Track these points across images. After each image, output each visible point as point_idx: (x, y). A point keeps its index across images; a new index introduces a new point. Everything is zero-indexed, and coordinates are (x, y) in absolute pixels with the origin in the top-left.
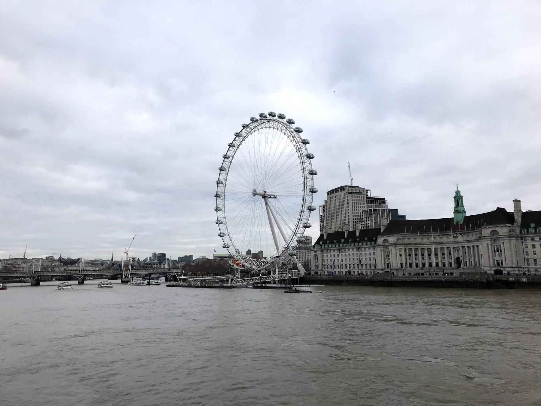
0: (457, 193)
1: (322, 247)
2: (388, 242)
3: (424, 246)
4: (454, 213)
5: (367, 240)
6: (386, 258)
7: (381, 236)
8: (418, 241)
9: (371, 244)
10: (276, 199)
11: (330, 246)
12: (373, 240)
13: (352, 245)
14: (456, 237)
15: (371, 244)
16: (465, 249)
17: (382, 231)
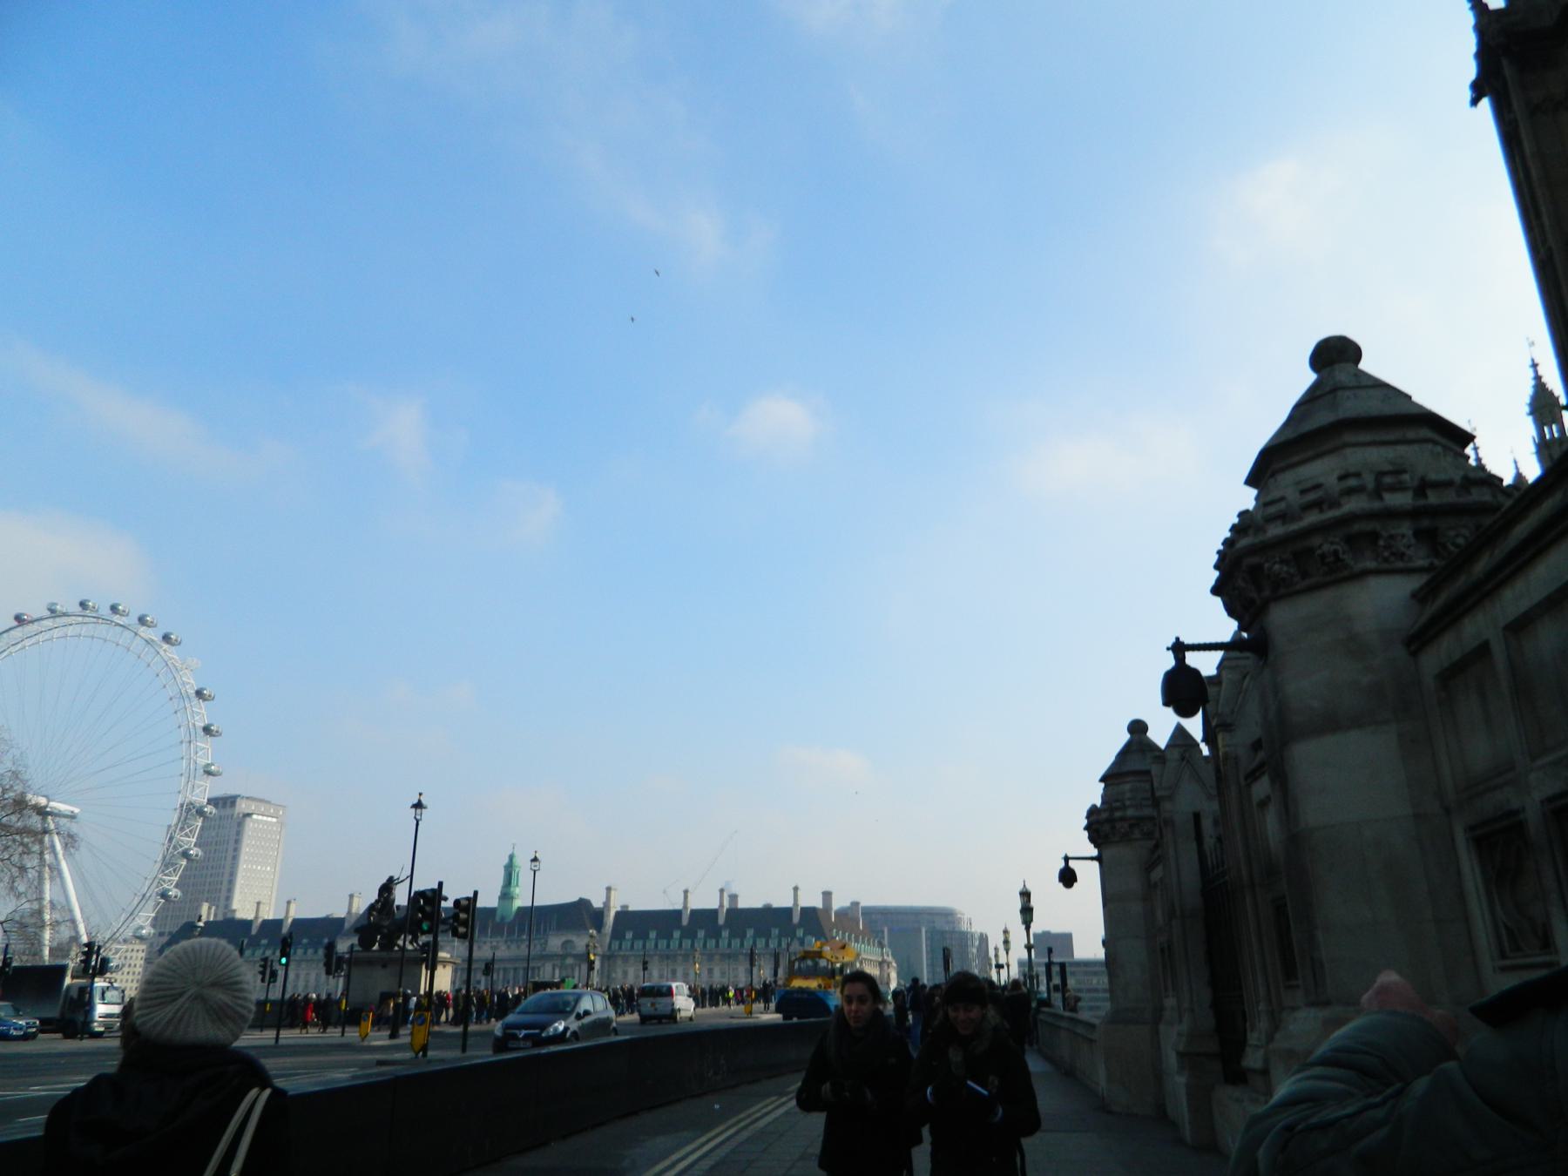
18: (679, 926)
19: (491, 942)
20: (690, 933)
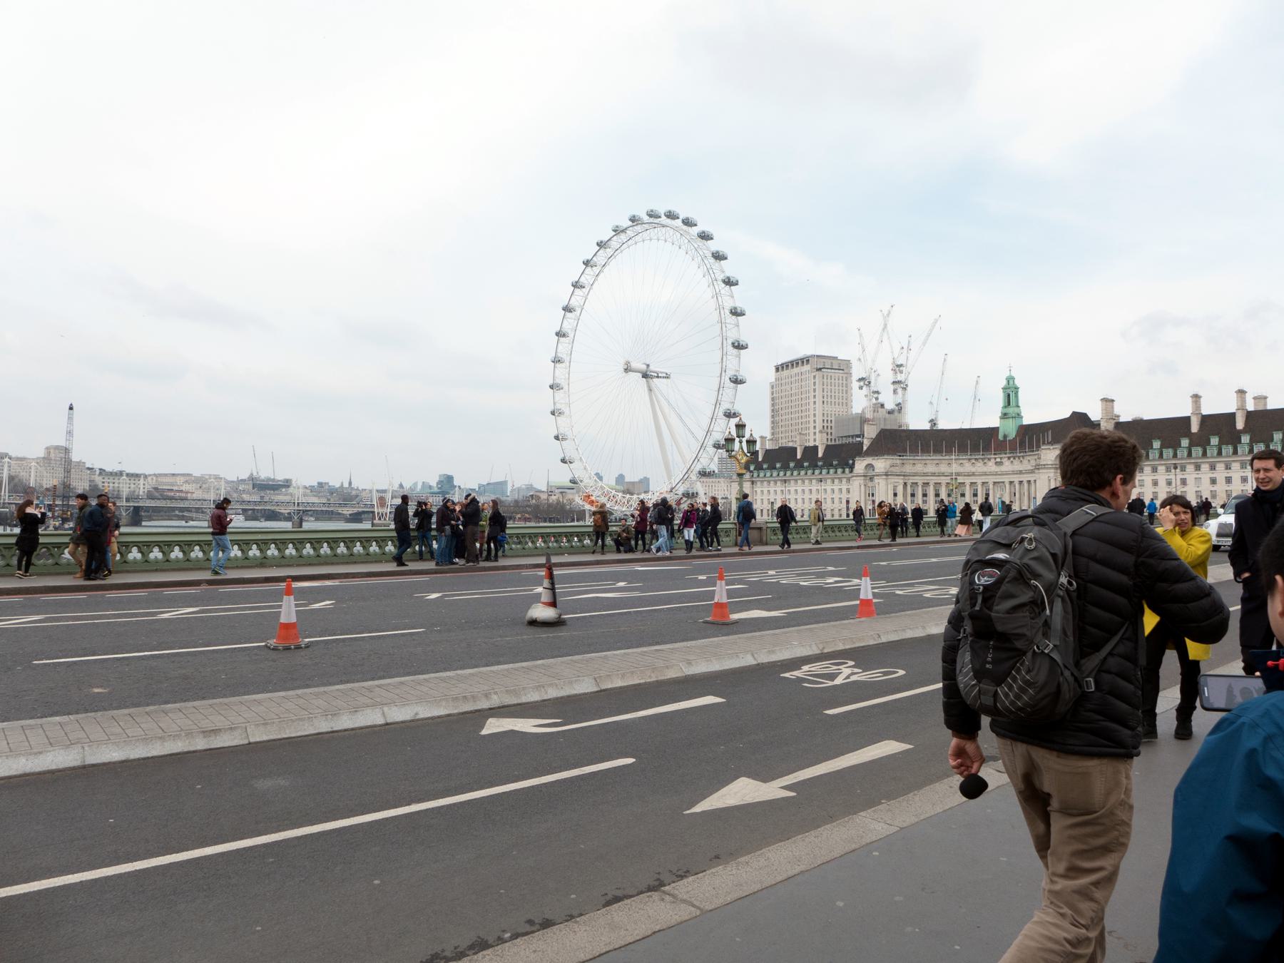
0: (1008, 381)
1: (753, 476)
2: (873, 470)
3: (940, 479)
4: (1001, 418)
5: (836, 465)
6: (869, 500)
7: (862, 459)
8: (931, 468)
9: (844, 472)
10: (668, 380)
11: (768, 474)
12: (847, 464)
13: (810, 472)
14: (1000, 464)
15: (844, 472)
16: (1015, 486)
17: (865, 448)
18: (1187, 433)
19: (995, 458)
20: (1200, 441)
